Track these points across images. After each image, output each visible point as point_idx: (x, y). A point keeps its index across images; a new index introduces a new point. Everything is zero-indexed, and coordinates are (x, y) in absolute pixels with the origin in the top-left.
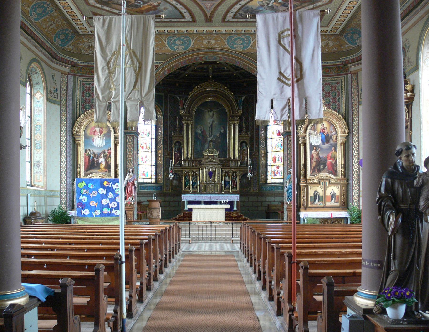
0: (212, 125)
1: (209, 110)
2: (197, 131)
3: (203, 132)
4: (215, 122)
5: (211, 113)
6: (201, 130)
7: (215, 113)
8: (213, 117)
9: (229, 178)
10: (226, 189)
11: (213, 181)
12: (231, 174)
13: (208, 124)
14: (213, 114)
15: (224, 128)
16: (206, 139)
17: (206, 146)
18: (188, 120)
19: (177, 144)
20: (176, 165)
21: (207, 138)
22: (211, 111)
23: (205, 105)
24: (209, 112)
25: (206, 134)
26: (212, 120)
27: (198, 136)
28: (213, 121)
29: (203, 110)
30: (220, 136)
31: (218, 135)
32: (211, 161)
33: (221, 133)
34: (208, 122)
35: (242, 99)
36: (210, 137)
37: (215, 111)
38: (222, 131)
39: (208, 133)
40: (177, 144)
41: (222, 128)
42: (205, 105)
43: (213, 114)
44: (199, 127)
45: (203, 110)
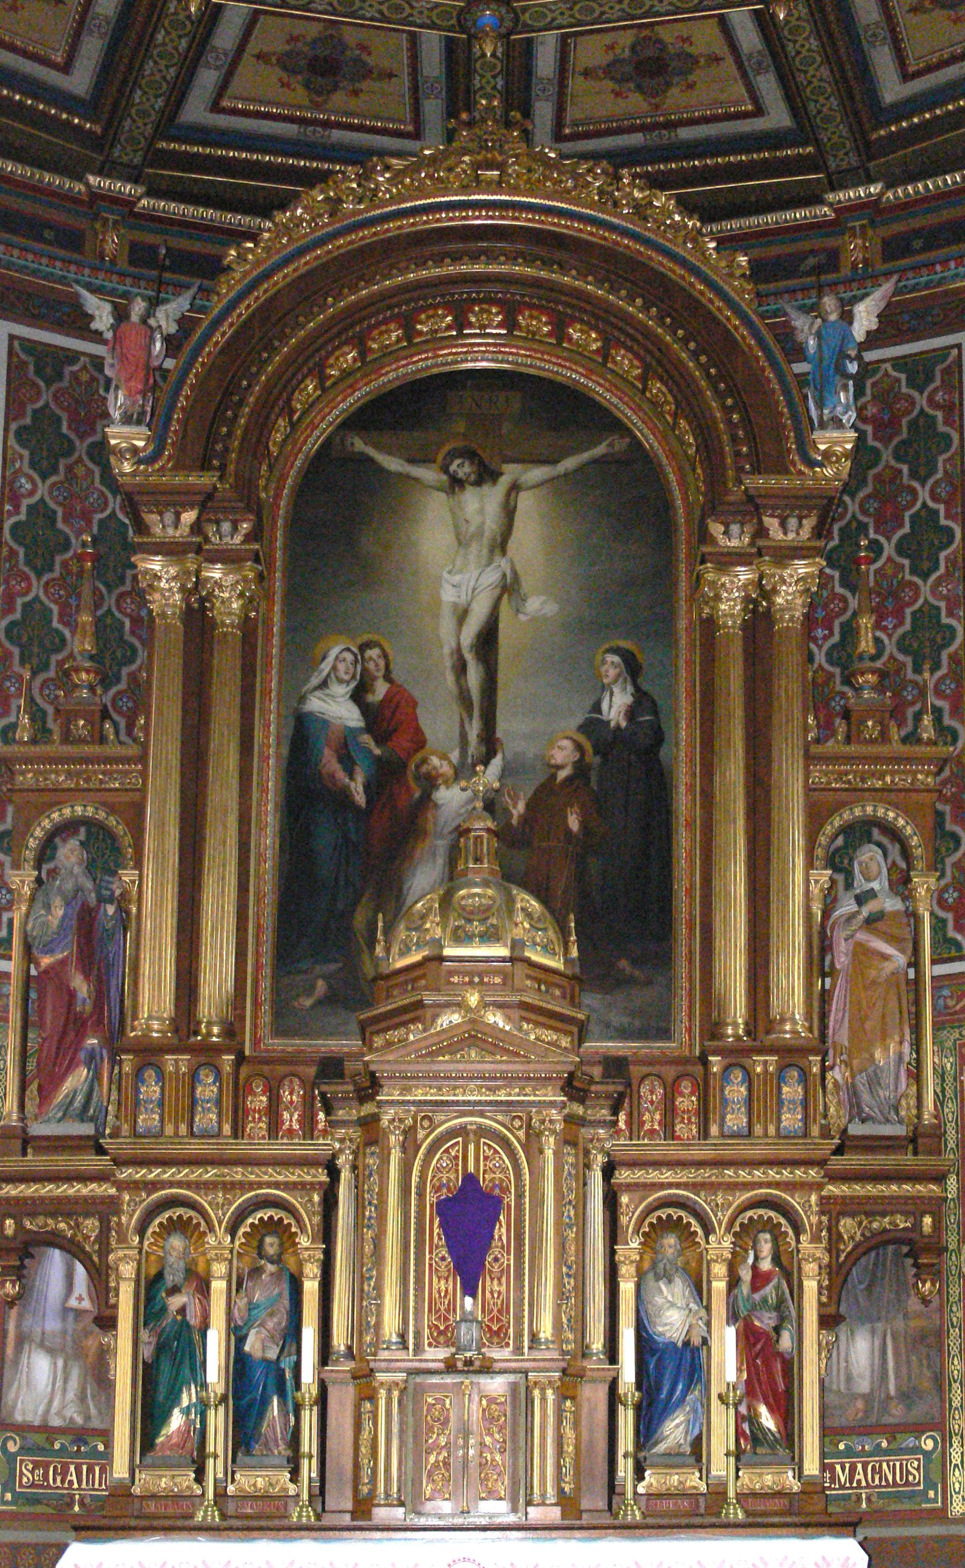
0: (488, 639)
1: (462, 468)
2: (315, 704)
3: (389, 719)
4: (534, 604)
5: (481, 505)
6: (358, 696)
7: (525, 501)
8: (501, 544)
9: (699, 1288)
10: (672, 1460)
11: (497, 1335)
12: (720, 1245)
13: (447, 625)
14: (509, 512)
15: (632, 667)
16: (426, 799)
17: (423, 880)
18: (197, 548)
19: (70, 854)
20: (37, 1129)
21: (430, 782)
22: (486, 474)
23: (411, 410)
24: (456, 484)
25: (420, 742)
26: (491, 577)
27: (330, 763)
28: (509, 588)
29: (393, 464)
30: (581, 768)
31: (563, 754)
32: (474, 1036)
33: (593, 726)
34: (448, 595)
35: (847, 317)
36: (463, 771)
37: (537, 473)
38: (616, 705)
39: (441, 727)
40: (70, 854)
41: (611, 665)
42: (411, 410)
43: (509, 512)
44: (337, 654)
45: (393, 464)
